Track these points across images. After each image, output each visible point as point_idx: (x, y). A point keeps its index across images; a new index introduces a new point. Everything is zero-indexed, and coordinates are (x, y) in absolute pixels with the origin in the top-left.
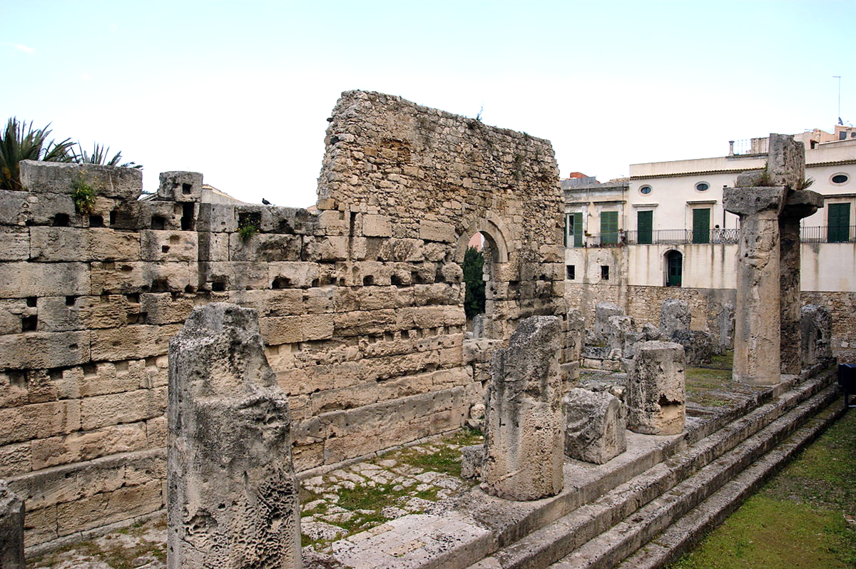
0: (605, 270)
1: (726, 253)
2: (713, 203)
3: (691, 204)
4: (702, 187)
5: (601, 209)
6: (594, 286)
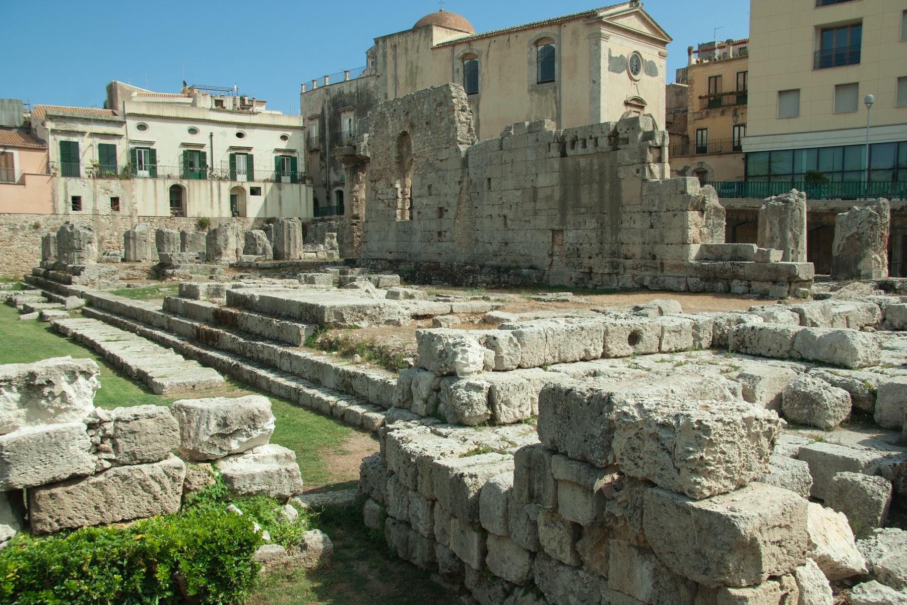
0: (115, 201)
1: (221, 188)
2: (202, 146)
3: (184, 145)
4: (193, 131)
5: (98, 141)
6: (105, 217)
